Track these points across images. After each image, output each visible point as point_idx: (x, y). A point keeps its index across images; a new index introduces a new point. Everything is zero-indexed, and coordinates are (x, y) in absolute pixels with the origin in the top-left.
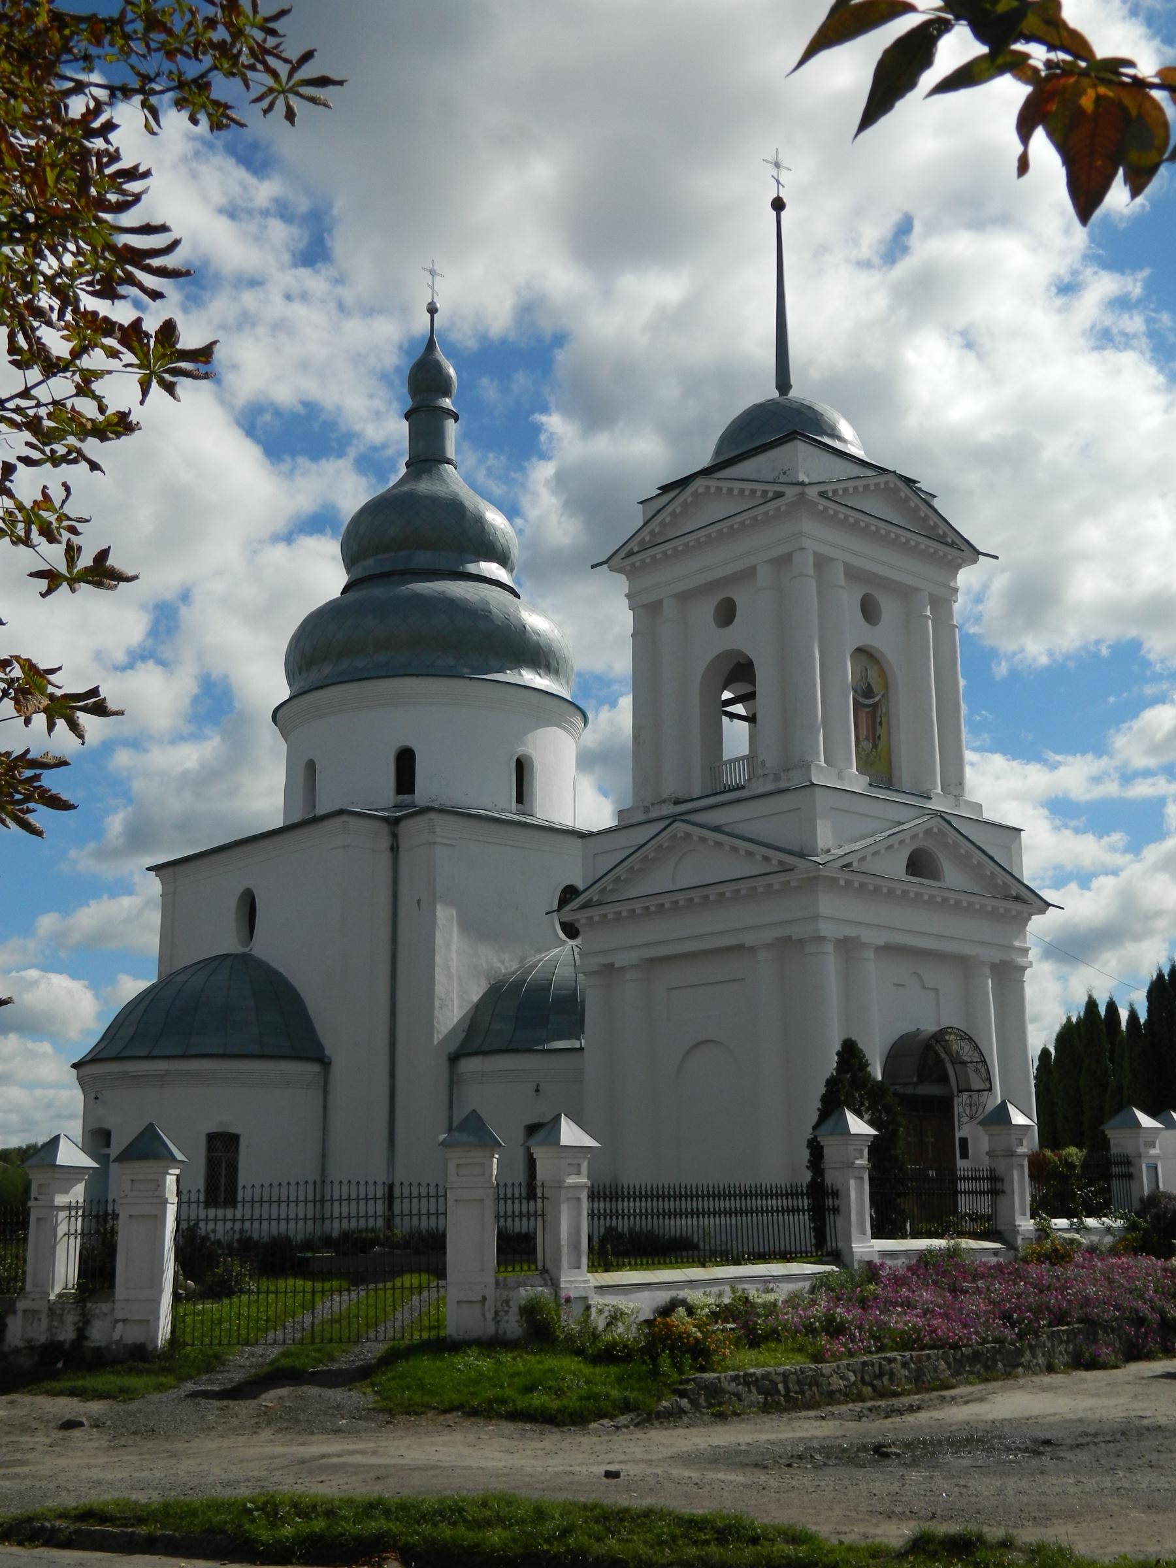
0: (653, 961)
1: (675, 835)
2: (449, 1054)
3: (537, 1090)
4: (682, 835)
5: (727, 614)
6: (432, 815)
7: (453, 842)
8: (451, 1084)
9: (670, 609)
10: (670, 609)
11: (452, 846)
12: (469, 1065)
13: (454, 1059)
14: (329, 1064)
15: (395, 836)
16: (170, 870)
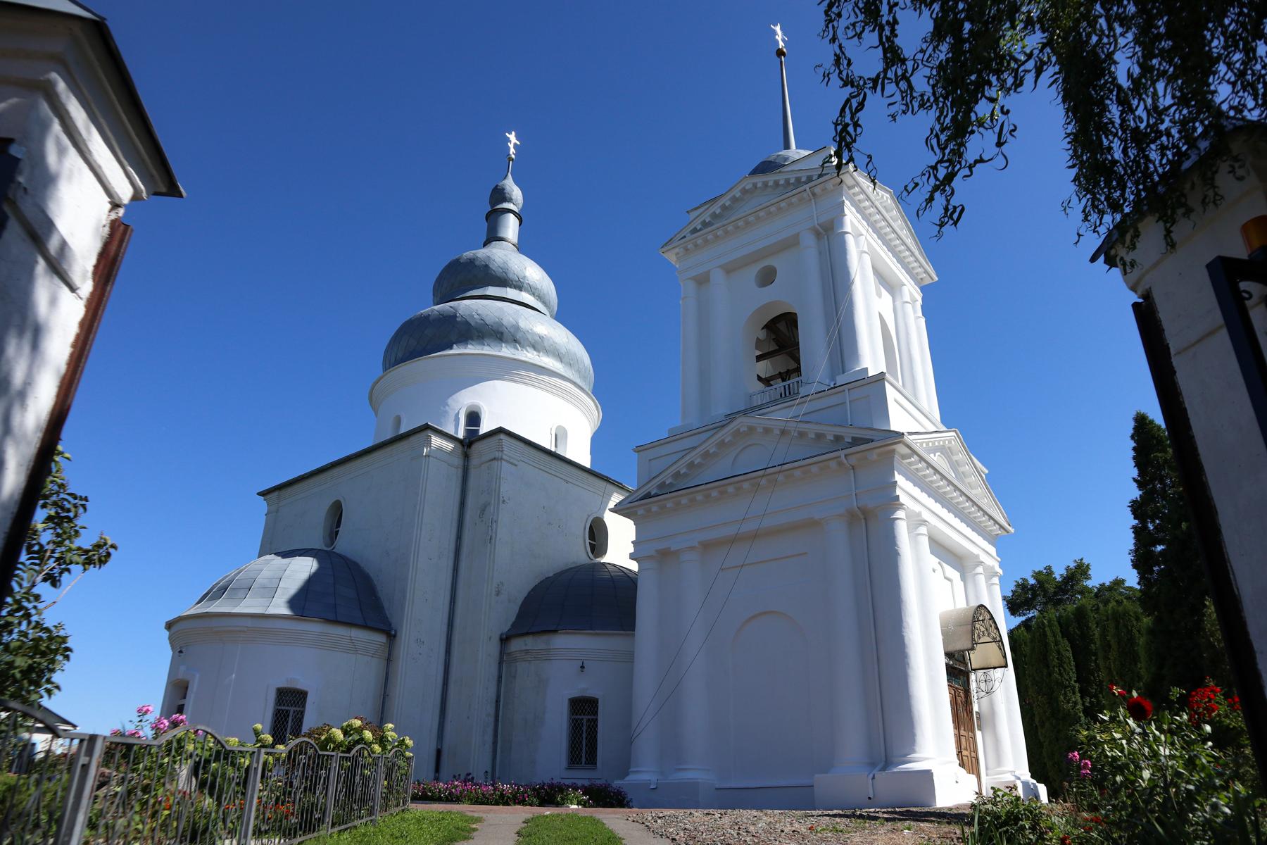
0: (707, 546)
1: (739, 430)
2: (501, 635)
3: (582, 667)
4: (746, 429)
5: (767, 277)
6: (502, 436)
7: (517, 463)
8: (501, 663)
9: (718, 277)
10: (718, 277)
11: (516, 465)
12: (516, 645)
13: (505, 640)
14: (395, 636)
15: (466, 456)
16: (276, 494)
